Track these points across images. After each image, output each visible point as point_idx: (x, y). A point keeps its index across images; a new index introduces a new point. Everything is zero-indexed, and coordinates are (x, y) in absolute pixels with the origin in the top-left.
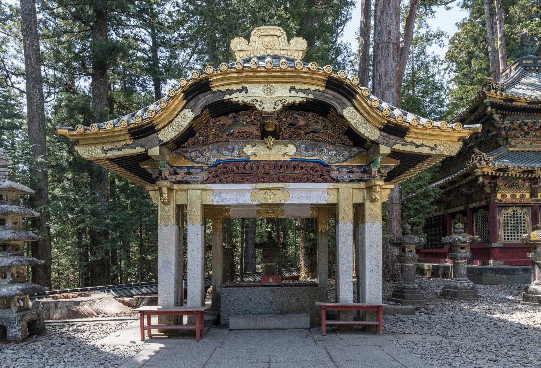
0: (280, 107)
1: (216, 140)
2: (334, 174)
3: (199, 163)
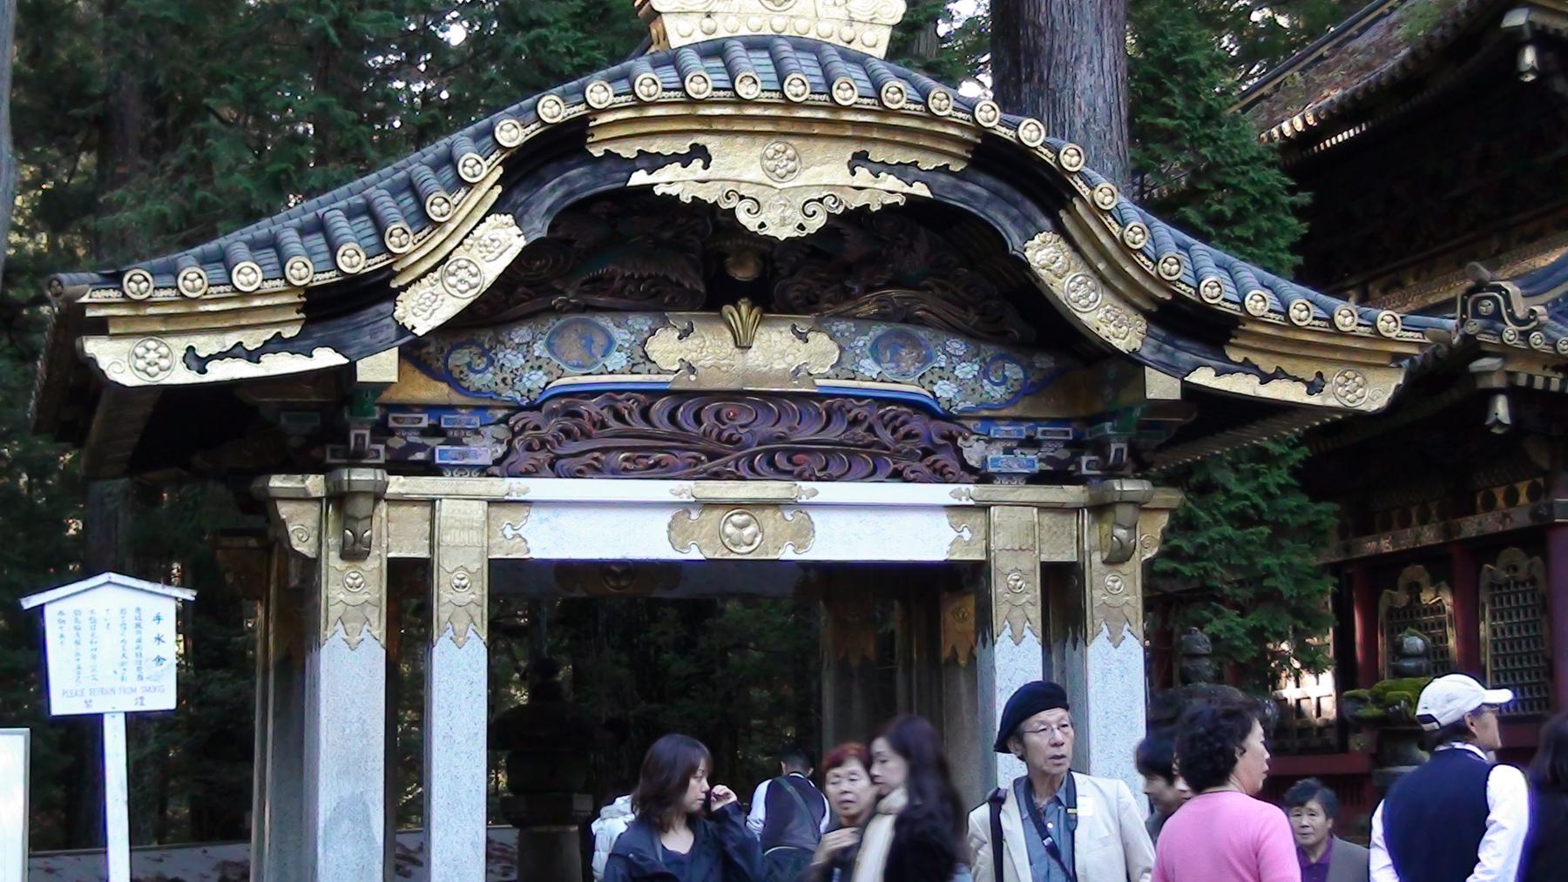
0: (818, 222)
1: (540, 303)
2: (974, 452)
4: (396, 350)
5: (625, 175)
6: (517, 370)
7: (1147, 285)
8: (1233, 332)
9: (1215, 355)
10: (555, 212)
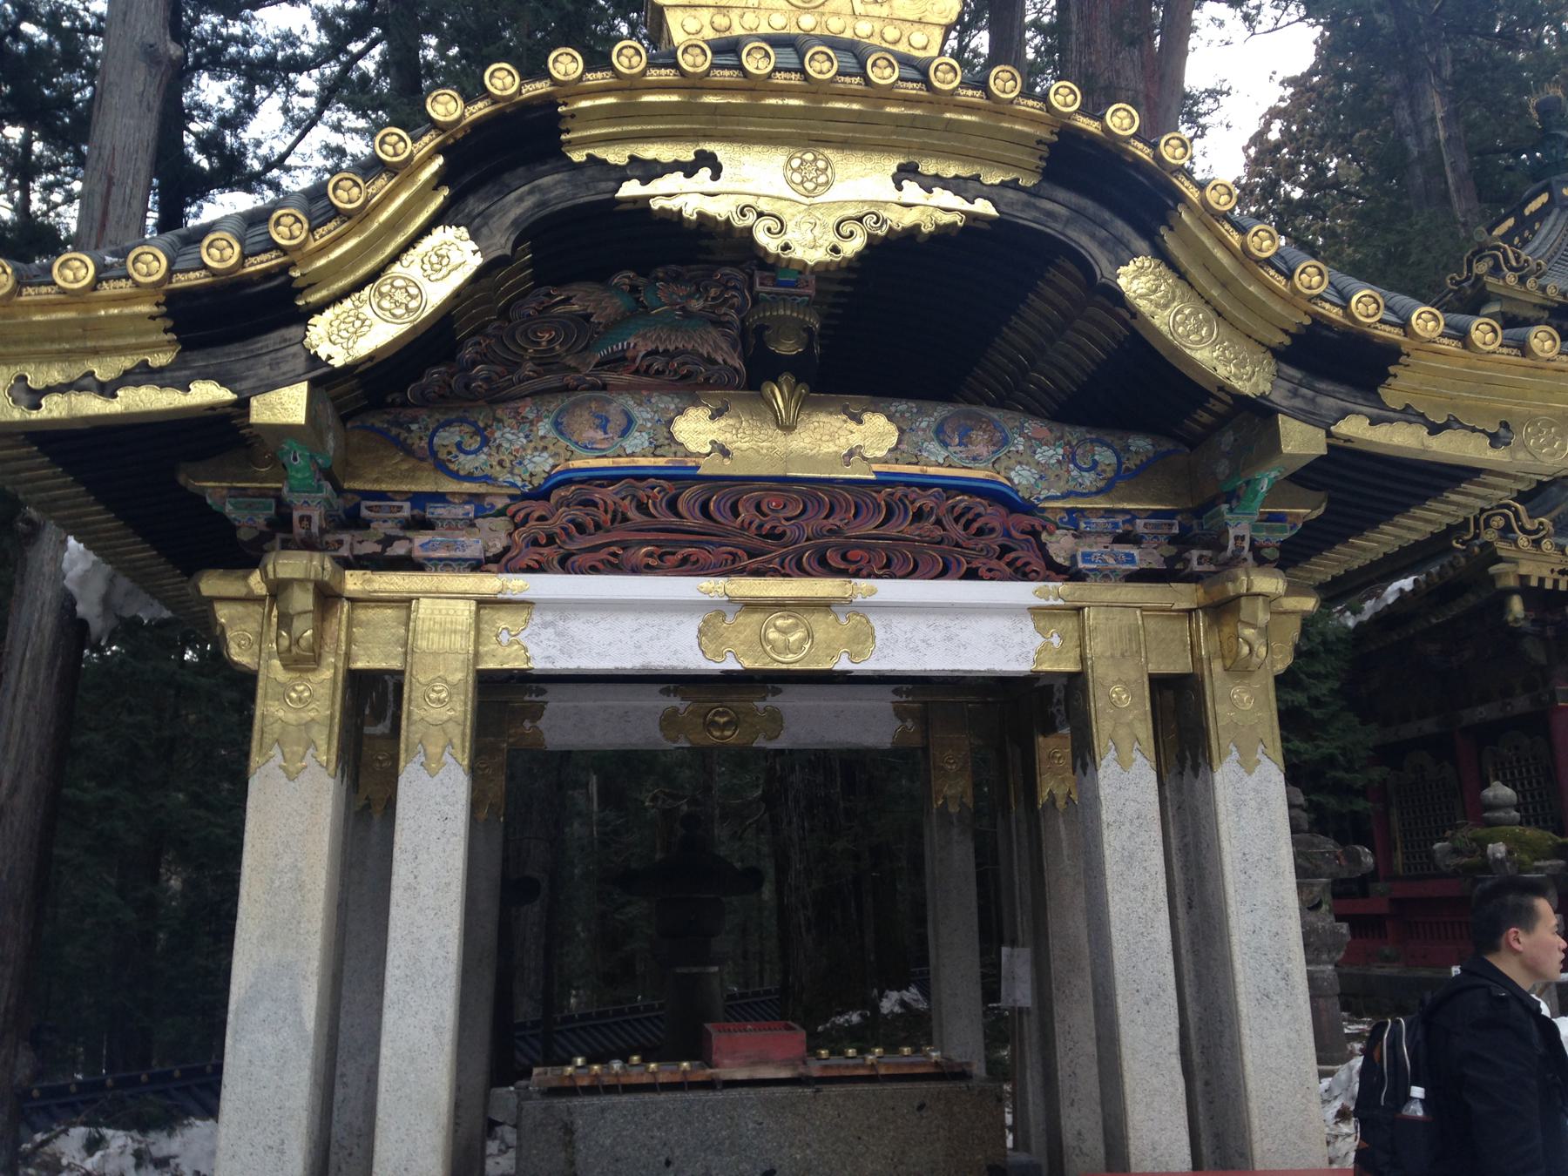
1: (551, 380)
2: (1060, 545)
3: (470, 477)
4: (303, 387)
5: (612, 184)
6: (517, 451)
7: (1277, 307)
8: (1392, 369)
9: (1365, 399)
10: (524, 226)
